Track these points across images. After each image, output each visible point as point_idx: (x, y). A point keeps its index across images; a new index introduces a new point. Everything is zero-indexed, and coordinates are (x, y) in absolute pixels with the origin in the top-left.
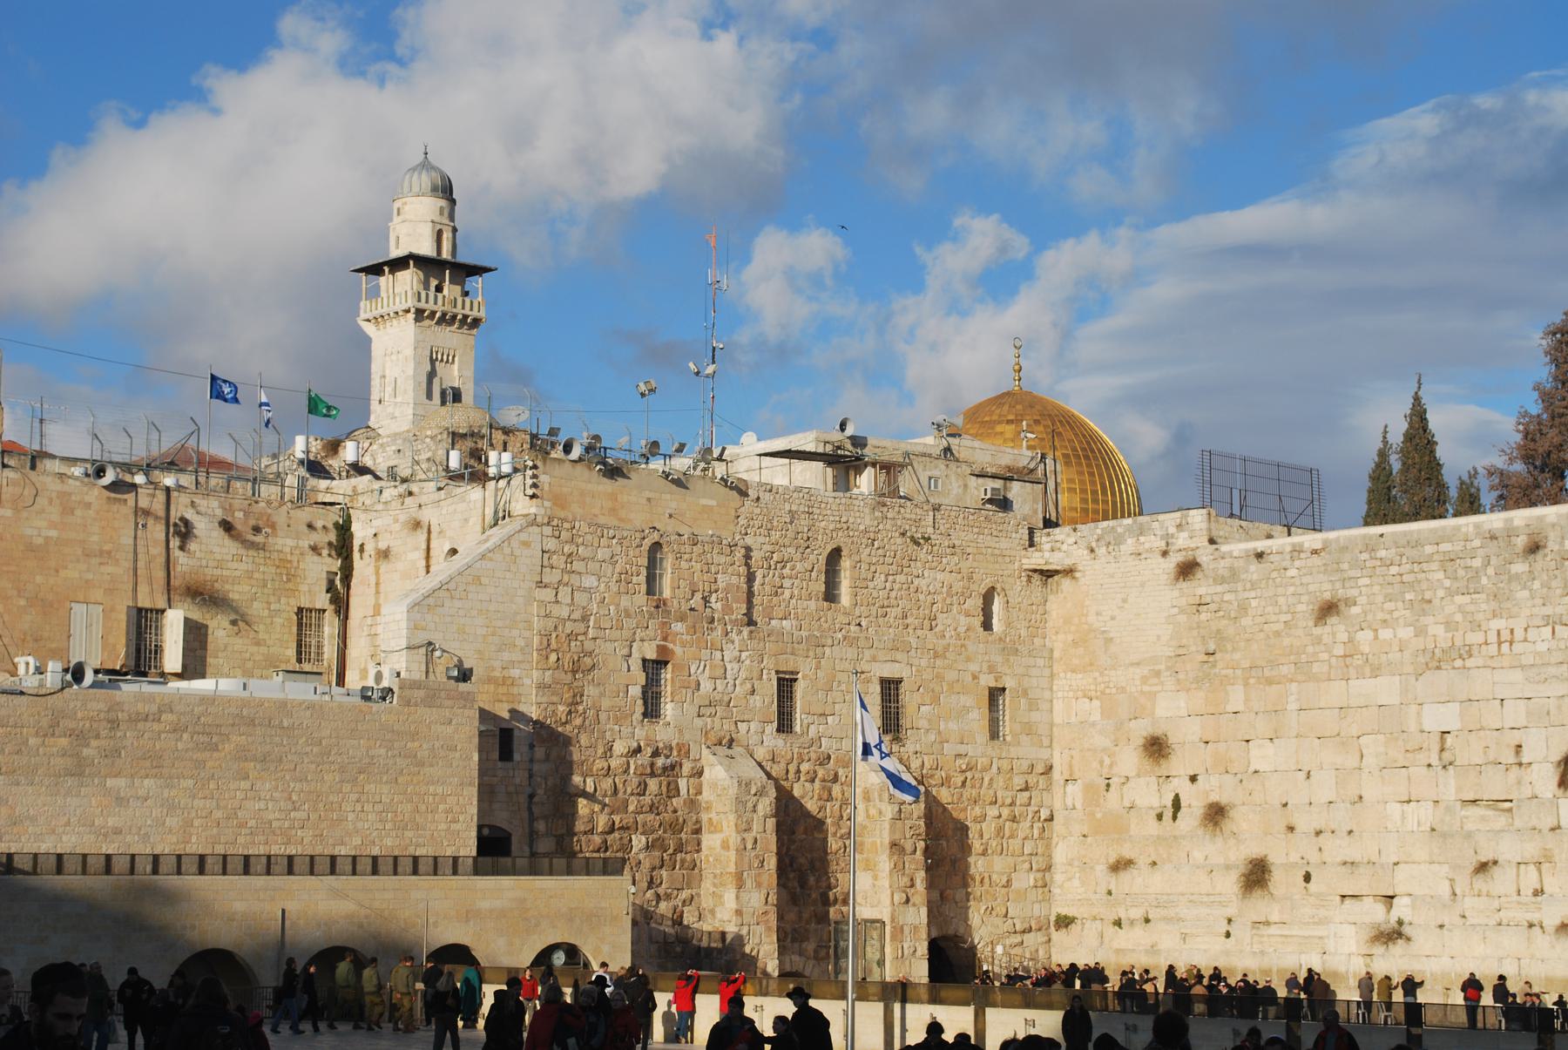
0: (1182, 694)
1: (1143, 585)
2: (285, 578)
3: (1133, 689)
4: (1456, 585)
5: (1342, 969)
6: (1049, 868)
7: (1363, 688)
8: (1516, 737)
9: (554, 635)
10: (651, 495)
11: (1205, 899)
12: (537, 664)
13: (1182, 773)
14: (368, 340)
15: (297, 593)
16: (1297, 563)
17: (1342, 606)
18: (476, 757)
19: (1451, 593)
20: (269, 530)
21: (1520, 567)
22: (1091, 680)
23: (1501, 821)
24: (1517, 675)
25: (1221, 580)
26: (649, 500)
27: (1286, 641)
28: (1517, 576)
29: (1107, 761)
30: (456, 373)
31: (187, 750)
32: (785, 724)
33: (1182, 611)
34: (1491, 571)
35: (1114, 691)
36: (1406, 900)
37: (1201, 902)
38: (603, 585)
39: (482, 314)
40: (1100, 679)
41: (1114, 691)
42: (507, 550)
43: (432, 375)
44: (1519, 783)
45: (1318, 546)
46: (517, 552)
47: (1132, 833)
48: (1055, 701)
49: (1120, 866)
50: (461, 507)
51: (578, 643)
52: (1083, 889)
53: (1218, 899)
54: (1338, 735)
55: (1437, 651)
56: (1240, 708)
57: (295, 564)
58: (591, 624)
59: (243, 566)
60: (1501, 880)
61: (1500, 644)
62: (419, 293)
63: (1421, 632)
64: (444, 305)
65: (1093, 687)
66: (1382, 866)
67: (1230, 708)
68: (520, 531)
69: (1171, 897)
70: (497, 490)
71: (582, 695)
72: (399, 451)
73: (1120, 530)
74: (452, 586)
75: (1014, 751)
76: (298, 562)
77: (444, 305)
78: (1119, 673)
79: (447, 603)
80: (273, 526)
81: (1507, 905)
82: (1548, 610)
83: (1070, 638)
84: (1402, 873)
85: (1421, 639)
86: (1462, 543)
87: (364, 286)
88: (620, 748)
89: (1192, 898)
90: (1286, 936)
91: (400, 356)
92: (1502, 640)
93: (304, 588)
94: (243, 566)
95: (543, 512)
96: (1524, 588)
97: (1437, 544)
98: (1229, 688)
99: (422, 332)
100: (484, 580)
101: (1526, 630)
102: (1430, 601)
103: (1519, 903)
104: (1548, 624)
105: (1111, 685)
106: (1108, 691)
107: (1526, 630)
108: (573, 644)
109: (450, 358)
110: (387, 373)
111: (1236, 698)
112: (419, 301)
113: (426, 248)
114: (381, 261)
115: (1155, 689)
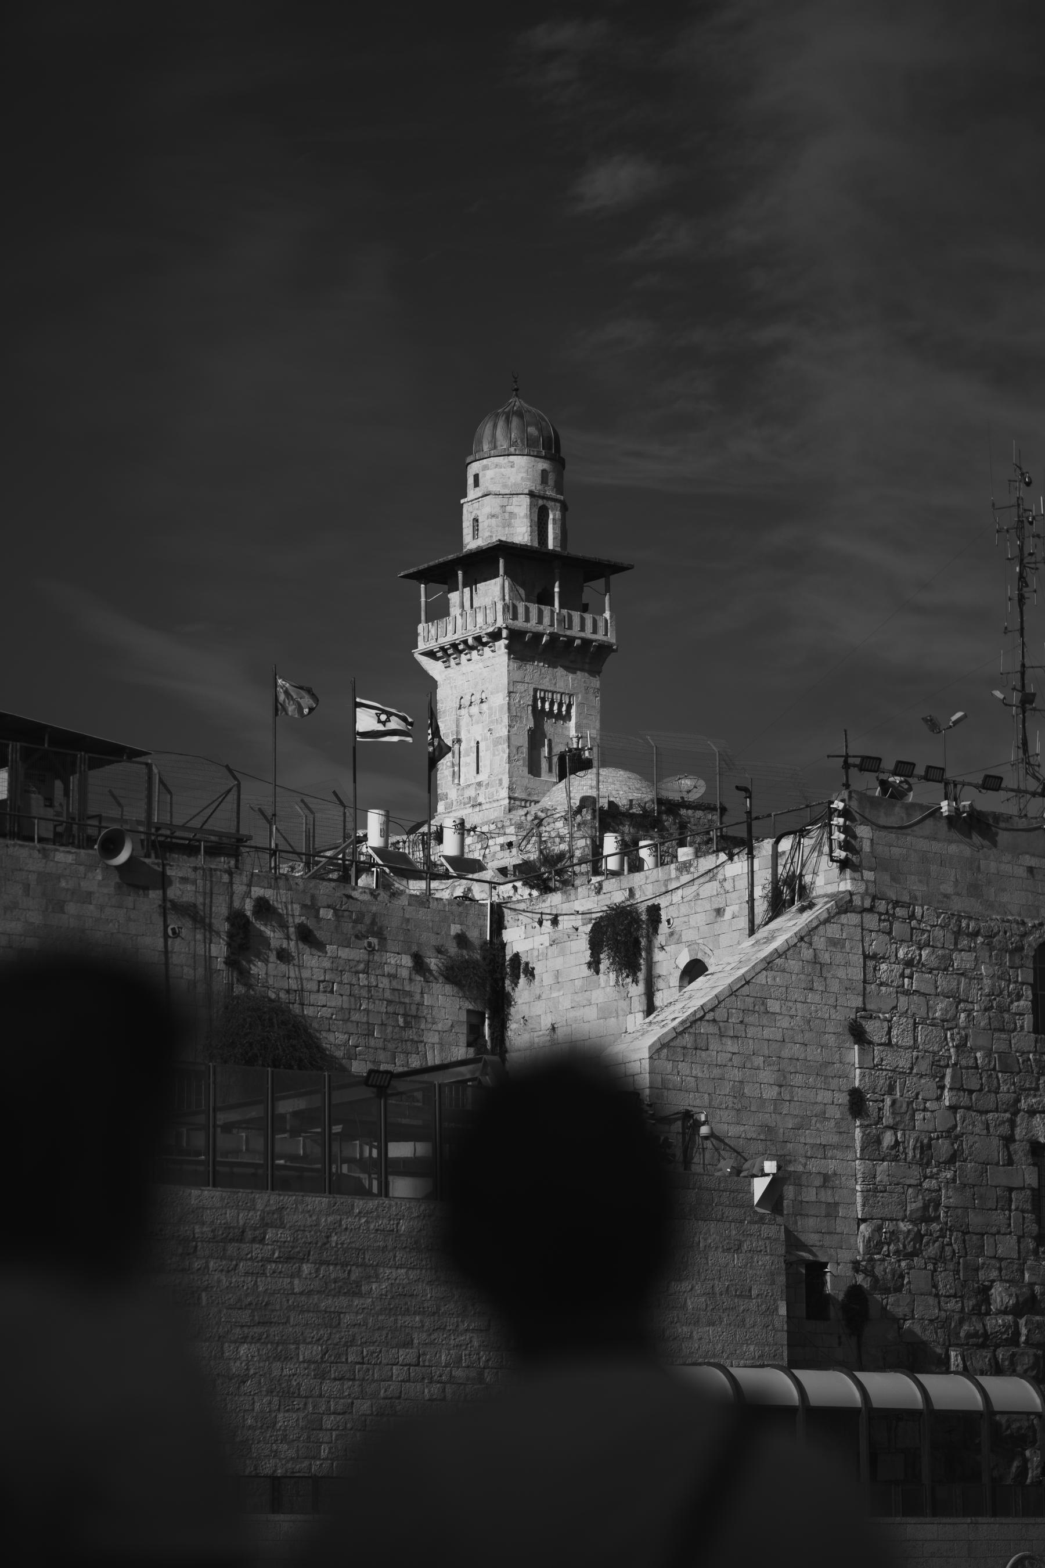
2: (401, 1020)
9: (888, 1101)
10: (1033, 862)
12: (862, 1150)
14: (432, 684)
15: (421, 1047)
18: (783, 1310)
20: (374, 941)
26: (1031, 870)
30: (573, 733)
31: (310, 1293)
38: (963, 1015)
39: (611, 638)
42: (807, 954)
43: (536, 738)
46: (825, 958)
50: (710, 888)
51: (928, 1114)
57: (417, 998)
58: (948, 1081)
59: (335, 1001)
62: (515, 607)
64: (552, 625)
68: (827, 921)
70: (776, 855)
71: (938, 1205)
72: (510, 845)
74: (720, 1014)
76: (422, 993)
77: (552, 625)
79: (714, 1045)
80: (380, 935)
87: (423, 599)
88: (1000, 1297)
91: (484, 706)
93: (432, 1038)
94: (335, 1001)
95: (862, 888)
99: (519, 668)
100: (774, 1006)
108: (919, 1116)
109: (564, 708)
110: (463, 736)
112: (515, 617)
113: (521, 534)
114: (451, 557)
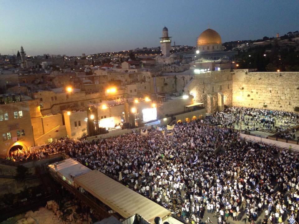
7: (263, 86)
8: (277, 91)
21: (279, 77)
23: (275, 98)
25: (249, 75)
32: (213, 91)
60: (275, 103)
63: (269, 81)
75: (229, 89)
84: (266, 101)
88: (202, 96)
111: (250, 85)
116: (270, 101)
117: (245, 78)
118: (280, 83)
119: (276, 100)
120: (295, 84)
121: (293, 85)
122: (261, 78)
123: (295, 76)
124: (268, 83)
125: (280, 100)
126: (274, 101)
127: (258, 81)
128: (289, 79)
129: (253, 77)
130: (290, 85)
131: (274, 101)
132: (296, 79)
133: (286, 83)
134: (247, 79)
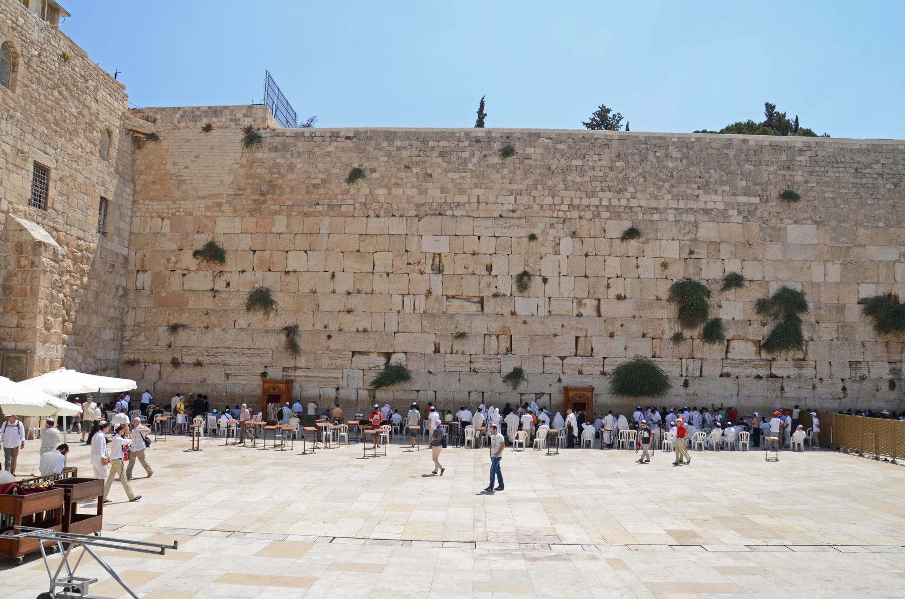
0: (238, 221)
1: (212, 147)
3: (199, 214)
4: (450, 167)
5: (353, 397)
6: (123, 327)
11: (247, 351)
13: (234, 269)
16: (334, 144)
17: (367, 173)
19: (446, 171)
21: (495, 160)
22: (164, 206)
24: (490, 223)
25: (276, 150)
27: (322, 191)
28: (493, 166)
29: (173, 259)
33: (242, 166)
34: (475, 160)
35: (183, 214)
36: (403, 356)
37: (243, 354)
40: (172, 206)
41: (183, 214)
44: (489, 285)
45: (352, 135)
47: (190, 307)
48: (134, 218)
49: (174, 329)
52: (147, 343)
53: (255, 351)
54: (358, 251)
55: (433, 204)
56: (283, 229)
60: (472, 346)
61: (478, 202)
63: (423, 192)
65: (166, 211)
66: (387, 334)
67: (274, 230)
69: (219, 350)
73: (197, 113)
78: (189, 202)
81: (475, 360)
82: (514, 187)
83: (150, 178)
84: (400, 337)
85: (423, 197)
86: (456, 143)
89: (235, 350)
90: (309, 377)
92: (480, 201)
96: (498, 172)
97: (438, 141)
98: (275, 217)
101: (497, 197)
102: (431, 175)
103: (485, 358)
104: (512, 195)
105: (181, 210)
106: (178, 214)
107: (497, 197)
115: (216, 214)
116: (432, 338)
117: (242, 171)
118: (509, 202)
119: (479, 326)
120: (607, 208)
121: (597, 215)
122: (366, 165)
123: (607, 155)
124: (418, 206)
125: (510, 322)
126: (461, 336)
127: (347, 192)
128: (566, 170)
129: (299, 163)
130: (575, 214)
131: (461, 336)
132: (611, 174)
133: (549, 200)
134: (254, 176)
